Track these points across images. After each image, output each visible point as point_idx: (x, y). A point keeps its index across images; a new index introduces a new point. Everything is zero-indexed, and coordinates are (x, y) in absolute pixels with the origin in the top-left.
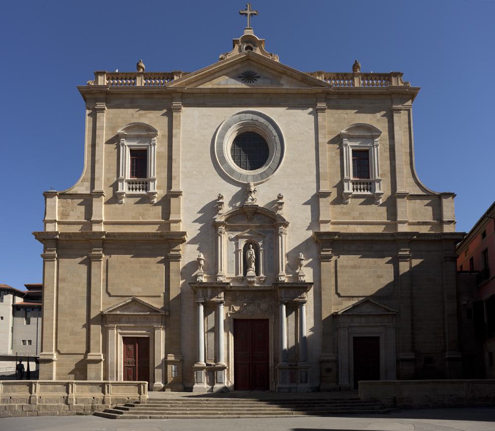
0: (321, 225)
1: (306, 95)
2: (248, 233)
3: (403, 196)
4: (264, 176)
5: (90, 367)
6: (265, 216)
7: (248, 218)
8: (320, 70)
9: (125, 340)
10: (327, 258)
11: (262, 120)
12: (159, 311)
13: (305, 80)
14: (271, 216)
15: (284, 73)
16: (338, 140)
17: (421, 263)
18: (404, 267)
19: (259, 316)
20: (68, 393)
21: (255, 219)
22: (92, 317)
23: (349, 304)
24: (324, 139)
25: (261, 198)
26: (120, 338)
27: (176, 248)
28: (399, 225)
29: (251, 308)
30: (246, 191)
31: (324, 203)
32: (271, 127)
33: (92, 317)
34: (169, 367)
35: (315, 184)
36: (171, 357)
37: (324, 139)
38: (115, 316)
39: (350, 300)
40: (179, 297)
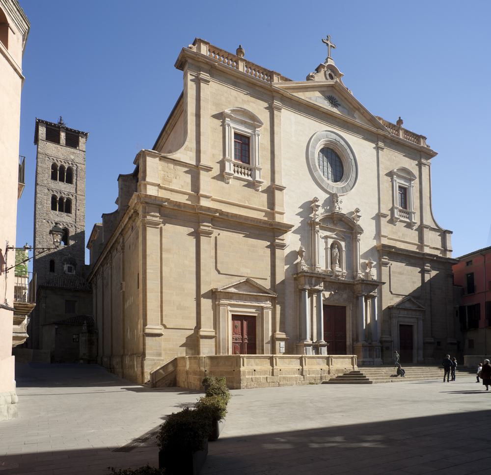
0: (382, 238)
1: (371, 133)
2: (335, 234)
3: (427, 227)
4: (344, 190)
5: (203, 342)
6: (346, 223)
7: (333, 222)
8: (381, 117)
9: (235, 317)
10: (386, 264)
11: (343, 143)
12: (268, 291)
13: (372, 120)
14: (351, 225)
15: (358, 110)
16: (390, 174)
17: (437, 274)
18: (427, 277)
19: (341, 304)
20: (302, 366)
21: (339, 224)
22: (203, 292)
23: (398, 300)
24: (383, 173)
25: (345, 206)
26: (230, 315)
27: (280, 238)
28: (425, 247)
29: (336, 297)
30: (333, 199)
31: (384, 221)
32: (348, 150)
33: (203, 292)
34: (277, 343)
35: (377, 206)
36: (280, 335)
37: (383, 173)
38: (227, 294)
39: (397, 297)
40: (283, 282)
